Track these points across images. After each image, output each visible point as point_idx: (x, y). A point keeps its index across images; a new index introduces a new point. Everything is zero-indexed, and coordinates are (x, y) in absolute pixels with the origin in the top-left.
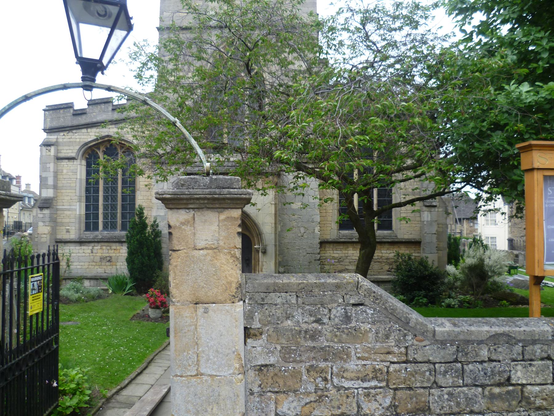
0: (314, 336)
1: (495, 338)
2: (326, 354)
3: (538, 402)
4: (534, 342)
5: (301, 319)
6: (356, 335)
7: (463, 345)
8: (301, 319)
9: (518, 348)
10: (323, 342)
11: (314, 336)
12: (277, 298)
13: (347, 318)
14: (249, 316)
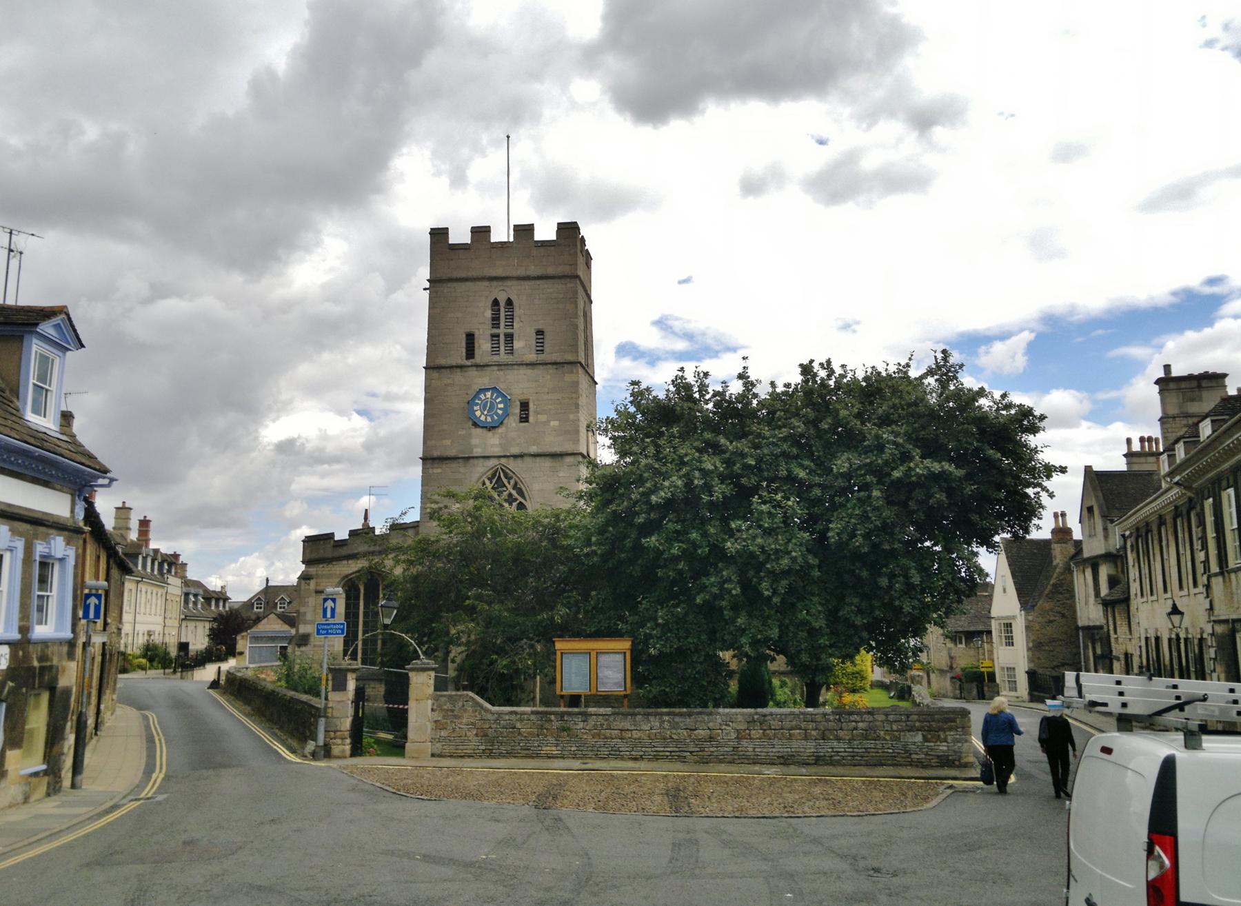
1: (511, 713)
2: (456, 717)
5: (448, 706)
6: (465, 711)
7: (500, 714)
8: (448, 706)
12: (443, 699)
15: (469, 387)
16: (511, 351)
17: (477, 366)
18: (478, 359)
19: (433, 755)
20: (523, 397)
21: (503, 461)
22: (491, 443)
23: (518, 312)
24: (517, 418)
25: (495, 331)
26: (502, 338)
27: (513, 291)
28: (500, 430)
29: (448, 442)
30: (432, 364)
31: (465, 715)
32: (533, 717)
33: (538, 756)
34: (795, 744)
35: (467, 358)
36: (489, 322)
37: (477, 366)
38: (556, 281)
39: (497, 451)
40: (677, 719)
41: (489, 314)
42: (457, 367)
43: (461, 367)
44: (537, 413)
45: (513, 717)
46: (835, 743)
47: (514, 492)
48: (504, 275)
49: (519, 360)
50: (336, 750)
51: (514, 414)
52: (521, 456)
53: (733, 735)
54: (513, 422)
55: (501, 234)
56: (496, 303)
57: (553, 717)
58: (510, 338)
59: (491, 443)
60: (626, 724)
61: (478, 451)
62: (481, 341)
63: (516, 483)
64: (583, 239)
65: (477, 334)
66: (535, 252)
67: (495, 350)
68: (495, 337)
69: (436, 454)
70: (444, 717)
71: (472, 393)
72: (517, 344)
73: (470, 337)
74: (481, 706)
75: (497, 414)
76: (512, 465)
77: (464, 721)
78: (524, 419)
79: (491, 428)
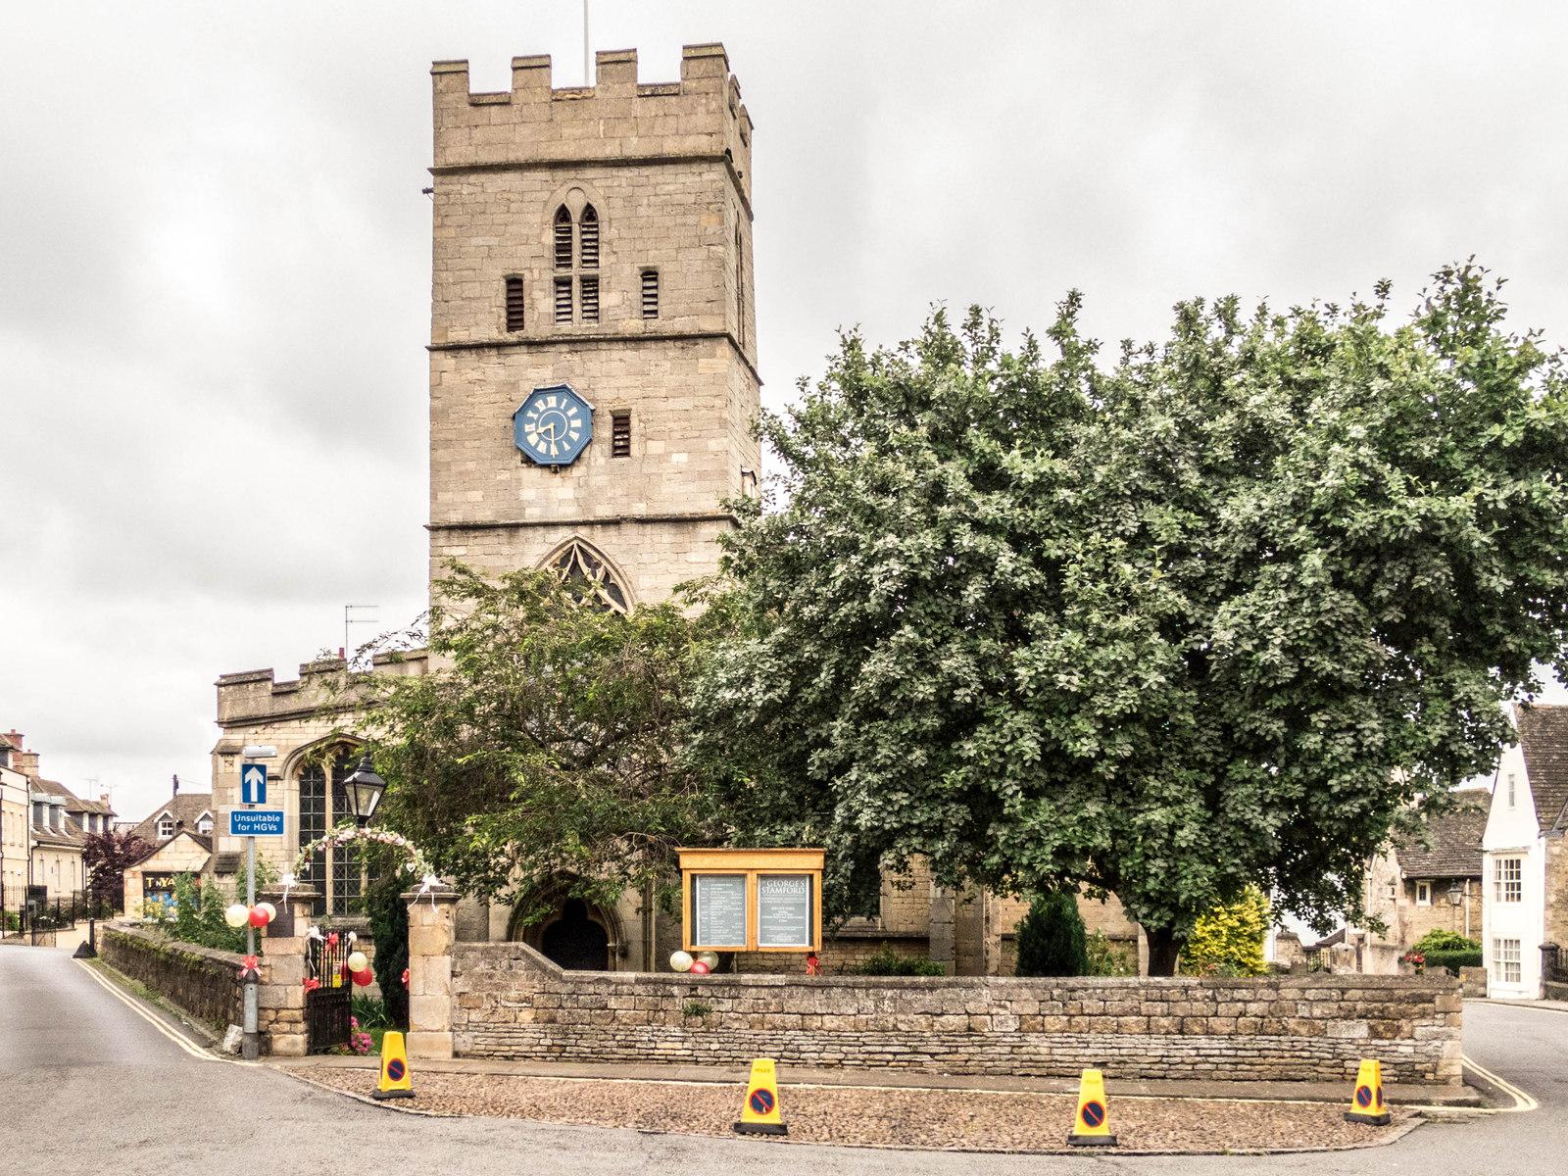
0: (491, 977)
1: (599, 981)
3: (624, 1020)
4: (623, 984)
5: (482, 967)
6: (514, 976)
8: (482, 967)
9: (613, 987)
10: (496, 980)
11: (491, 977)
12: (471, 955)
13: (511, 967)
14: (454, 965)
15: (514, 386)
16: (594, 314)
17: (530, 344)
18: (532, 329)
19: (456, 1055)
20: (618, 406)
21: (583, 532)
22: (557, 497)
23: (606, 233)
24: (607, 448)
25: (563, 272)
26: (576, 286)
27: (597, 188)
28: (577, 472)
29: (476, 496)
30: (441, 342)
31: (515, 985)
32: (639, 989)
33: (649, 1058)
34: (1126, 1041)
35: (510, 329)
36: (549, 254)
37: (530, 344)
38: (680, 168)
39: (571, 513)
40: (909, 995)
41: (549, 238)
42: (490, 346)
43: (499, 346)
44: (647, 438)
45: (602, 989)
46: (1203, 1041)
47: (604, 593)
48: (577, 157)
49: (610, 332)
50: (281, 1043)
51: (601, 441)
52: (616, 522)
53: (1013, 1025)
54: (599, 455)
55: (571, 71)
56: (563, 214)
57: (676, 990)
58: (591, 285)
59: (557, 497)
60: (815, 1002)
61: (532, 514)
62: (537, 294)
63: (607, 576)
64: (735, 86)
65: (527, 277)
66: (638, 107)
67: (563, 311)
68: (563, 283)
69: (455, 518)
70: (475, 987)
71: (521, 398)
72: (607, 300)
73: (514, 284)
74: (544, 970)
75: (569, 440)
76: (600, 539)
77: (513, 994)
78: (621, 450)
79: (559, 468)
